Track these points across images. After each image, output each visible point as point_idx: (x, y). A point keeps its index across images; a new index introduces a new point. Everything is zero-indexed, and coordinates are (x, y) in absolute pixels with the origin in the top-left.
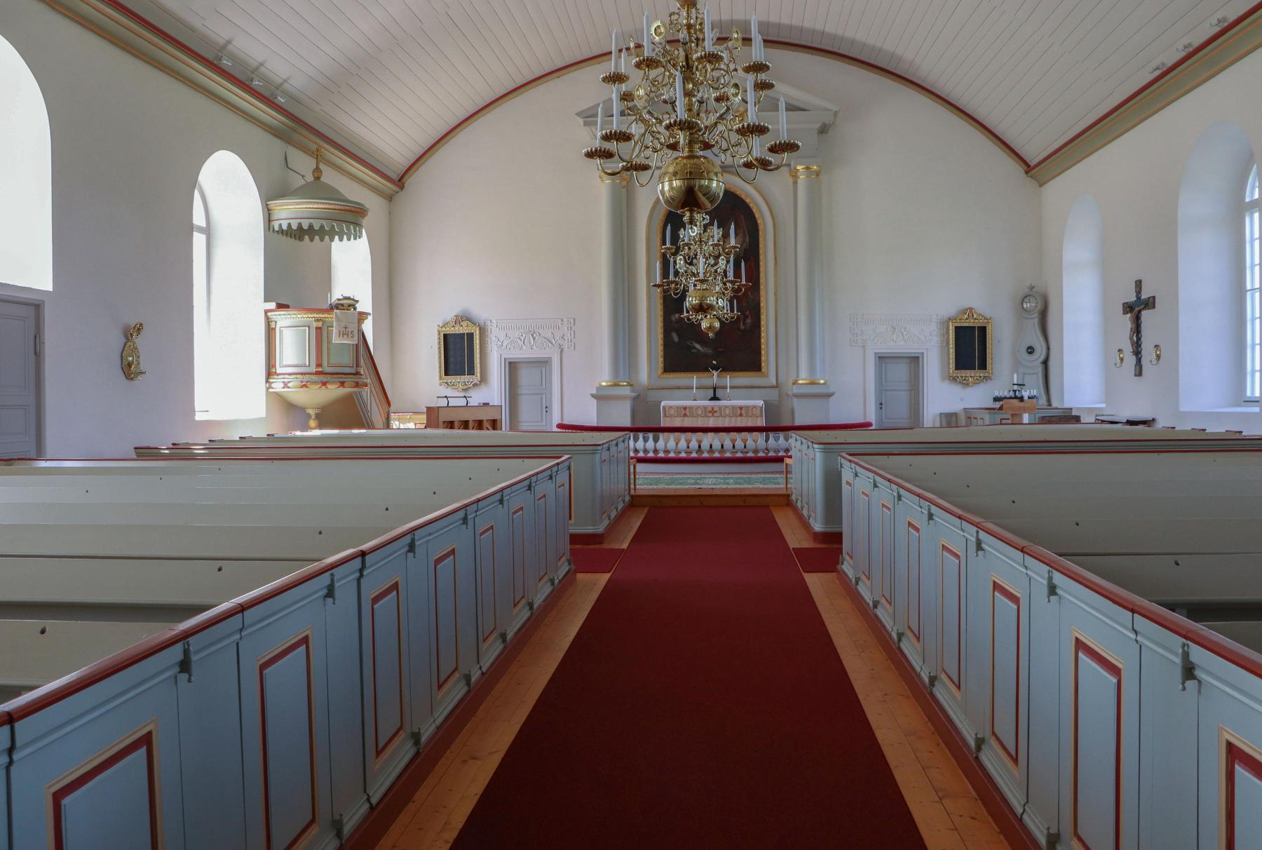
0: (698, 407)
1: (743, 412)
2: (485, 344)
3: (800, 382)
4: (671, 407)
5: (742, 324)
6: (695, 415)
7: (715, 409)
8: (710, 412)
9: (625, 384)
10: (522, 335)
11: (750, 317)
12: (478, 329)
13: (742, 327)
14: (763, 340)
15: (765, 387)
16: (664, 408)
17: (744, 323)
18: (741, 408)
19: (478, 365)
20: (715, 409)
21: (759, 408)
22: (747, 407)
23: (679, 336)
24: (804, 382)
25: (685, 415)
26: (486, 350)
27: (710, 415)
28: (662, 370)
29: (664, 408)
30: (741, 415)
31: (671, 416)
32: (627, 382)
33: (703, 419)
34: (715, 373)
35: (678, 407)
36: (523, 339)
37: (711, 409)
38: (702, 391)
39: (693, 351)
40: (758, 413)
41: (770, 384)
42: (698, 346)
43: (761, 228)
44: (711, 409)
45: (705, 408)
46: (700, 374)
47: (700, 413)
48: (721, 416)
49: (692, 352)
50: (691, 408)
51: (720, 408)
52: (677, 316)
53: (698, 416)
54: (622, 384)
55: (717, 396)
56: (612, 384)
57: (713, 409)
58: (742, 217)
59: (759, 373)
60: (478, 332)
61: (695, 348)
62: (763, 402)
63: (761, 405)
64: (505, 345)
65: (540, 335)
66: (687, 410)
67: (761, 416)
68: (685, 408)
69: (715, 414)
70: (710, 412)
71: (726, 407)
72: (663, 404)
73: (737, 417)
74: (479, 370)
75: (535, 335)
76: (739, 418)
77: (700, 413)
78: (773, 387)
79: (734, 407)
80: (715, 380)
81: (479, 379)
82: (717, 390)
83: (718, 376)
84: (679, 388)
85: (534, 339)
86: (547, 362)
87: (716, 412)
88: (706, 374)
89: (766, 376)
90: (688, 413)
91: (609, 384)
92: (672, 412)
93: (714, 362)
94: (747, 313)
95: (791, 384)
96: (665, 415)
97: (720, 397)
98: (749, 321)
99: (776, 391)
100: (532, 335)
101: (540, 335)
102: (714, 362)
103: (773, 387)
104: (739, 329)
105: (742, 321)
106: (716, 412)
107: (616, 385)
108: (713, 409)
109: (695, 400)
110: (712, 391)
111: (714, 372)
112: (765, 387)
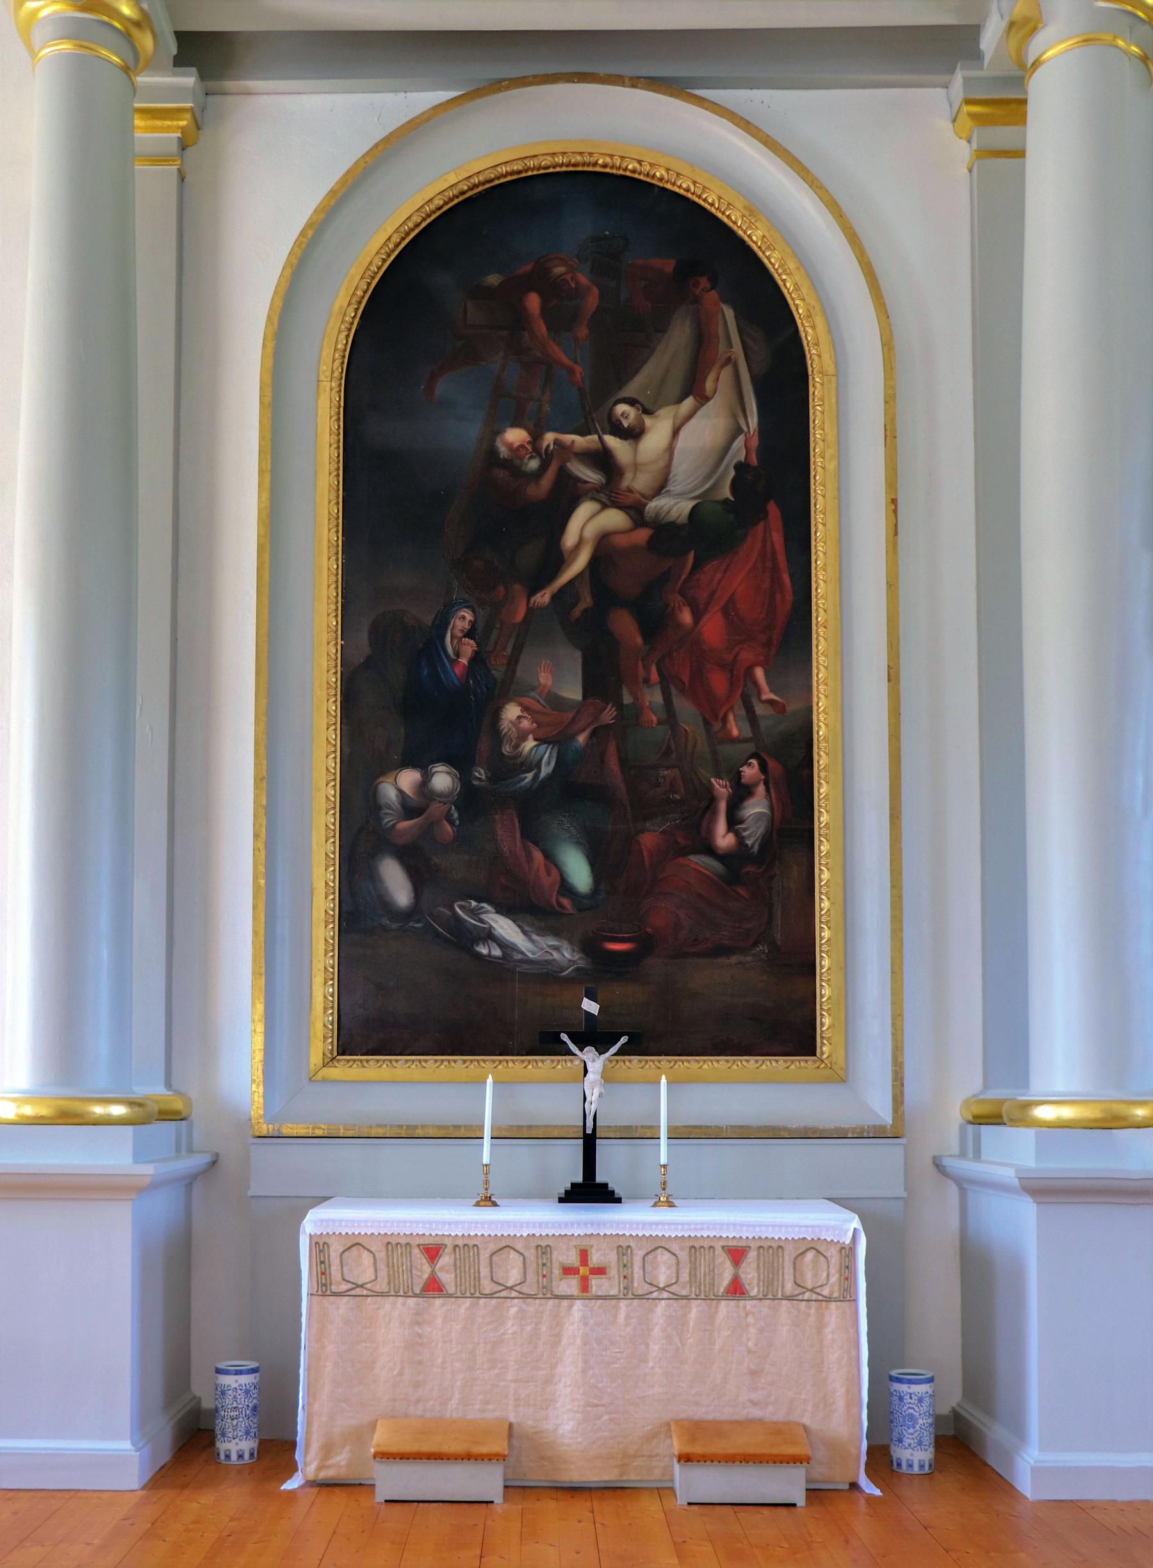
0: (505, 1246)
1: (749, 1273)
3: (1044, 1113)
4: (355, 1244)
5: (721, 826)
6: (488, 1287)
7: (595, 1259)
8: (568, 1271)
9: (118, 1110)
11: (761, 789)
13: (724, 839)
14: (823, 904)
15: (840, 1135)
16: (320, 1246)
17: (733, 822)
18: (737, 1254)
20: (595, 1259)
21: (833, 1254)
22: (772, 1250)
23: (418, 876)
24: (1067, 1113)
25: (433, 1287)
27: (570, 1286)
28: (331, 1044)
29: (320, 1246)
30: (736, 1289)
31: (357, 1291)
32: (130, 1103)
33: (532, 1307)
34: (595, 1062)
35: (394, 1246)
37: (573, 1259)
38: (524, 1154)
39: (483, 950)
40: (832, 1284)
41: (866, 1121)
42: (505, 927)
43: (818, 359)
44: (573, 1259)
45: (544, 1249)
46: (515, 1065)
47: (514, 1276)
48: (628, 1293)
49: (479, 956)
50: (466, 1248)
51: (624, 1250)
52: (408, 779)
53: (502, 1292)
54: (98, 1110)
55: (600, 1178)
56: (44, 1111)
57: (584, 1255)
58: (729, 313)
59: (799, 1064)
61: (489, 936)
62: (856, 1223)
63: (848, 1241)
66: (445, 1260)
67: (848, 1295)
68: (432, 1252)
69: (597, 1285)
70: (568, 1271)
71: (657, 1245)
72: (314, 1222)
73: (711, 1297)
76: (725, 1308)
77: (513, 1276)
78: (878, 1134)
79: (696, 1248)
80: (593, 1095)
82: (603, 1149)
83: (607, 1078)
84: (409, 1134)
87: (600, 1271)
88: (545, 1065)
89: (840, 1076)
90: (447, 1278)
91: (29, 1110)
92: (364, 1269)
93: (590, 1006)
94: (750, 772)
95: (955, 1115)
96: (324, 1288)
97: (619, 1191)
98: (756, 808)
99: (889, 1154)
102: (590, 1006)
103: (878, 1134)
104: (709, 849)
105: (722, 806)
106: (600, 1271)
107: (68, 1117)
108: (584, 1255)
109: (488, 1201)
110: (576, 1148)
111: (589, 1054)
112: (840, 1135)
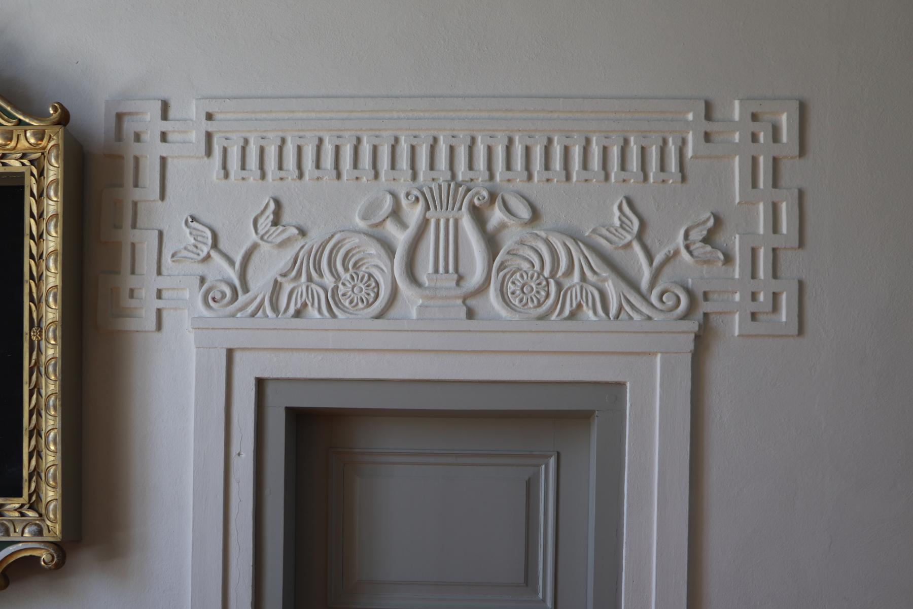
2: (114, 270)
10: (396, 213)
12: (54, 140)
19: (51, 422)
26: (121, 313)
36: (401, 238)
60: (54, 171)
64: (260, 282)
65: (536, 215)
74: (52, 458)
75: (497, 216)
81: (54, 528)
85: (492, 243)
86: (584, 417)
100: (478, 216)
101: (536, 215)
